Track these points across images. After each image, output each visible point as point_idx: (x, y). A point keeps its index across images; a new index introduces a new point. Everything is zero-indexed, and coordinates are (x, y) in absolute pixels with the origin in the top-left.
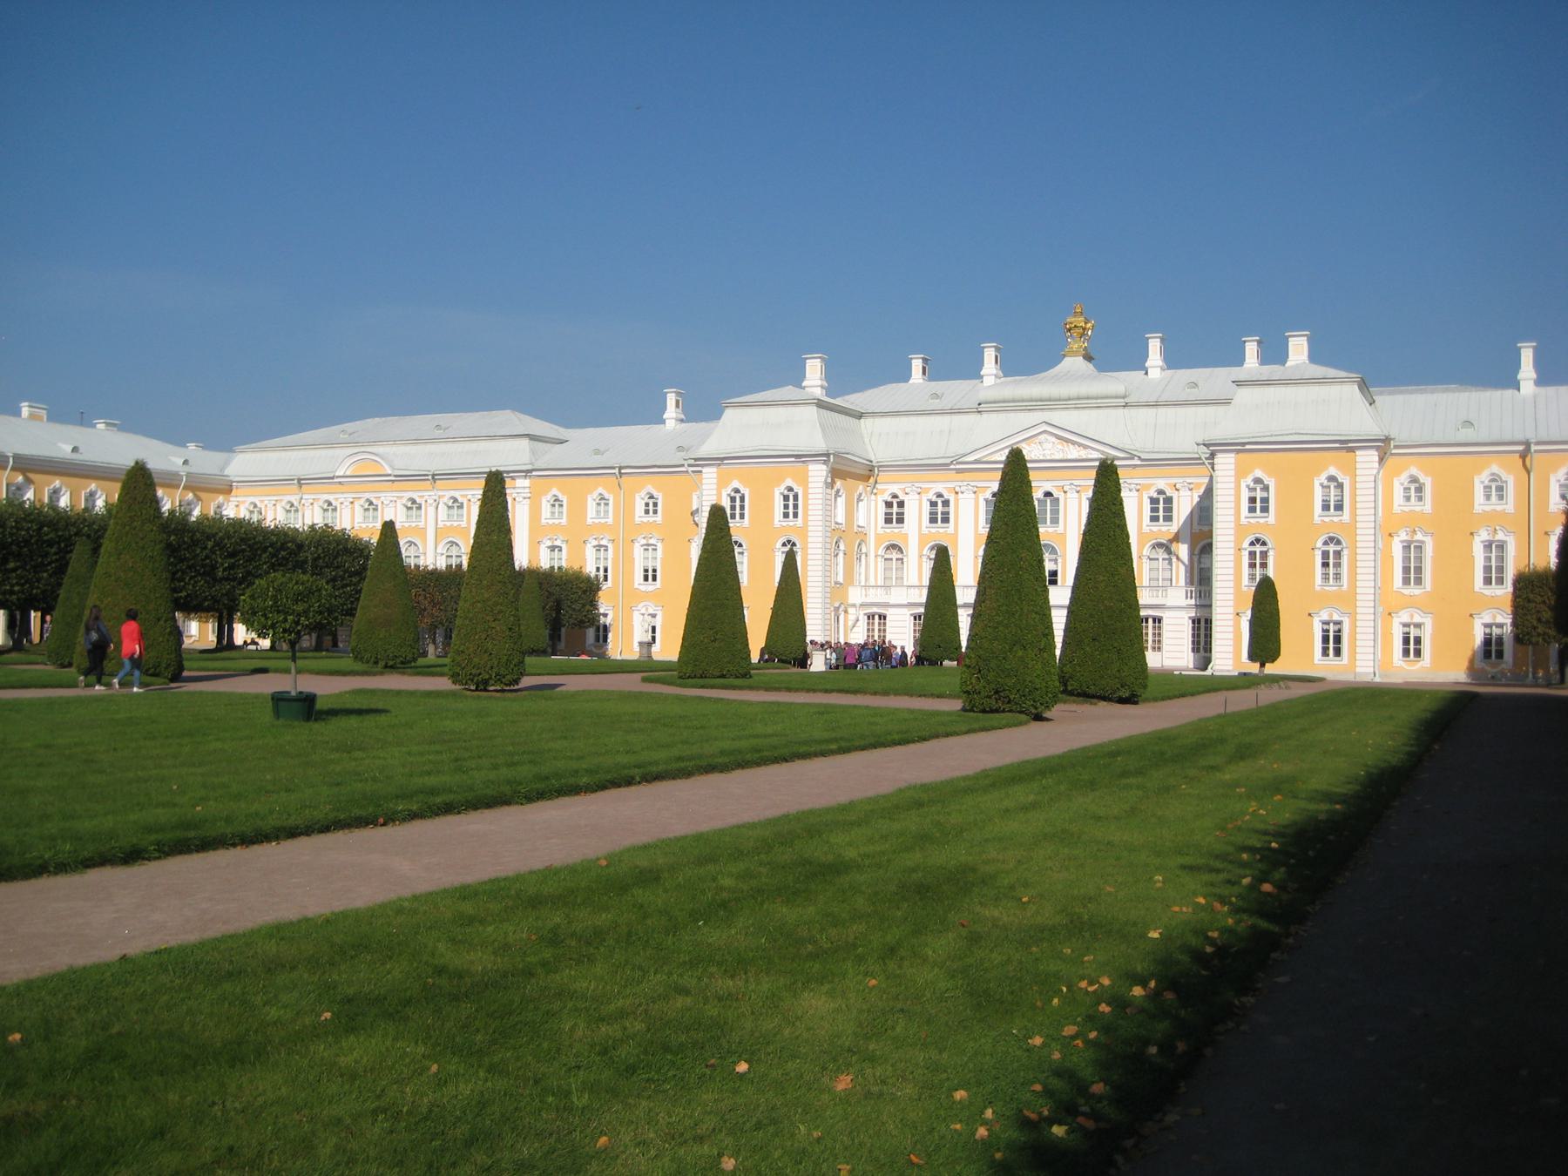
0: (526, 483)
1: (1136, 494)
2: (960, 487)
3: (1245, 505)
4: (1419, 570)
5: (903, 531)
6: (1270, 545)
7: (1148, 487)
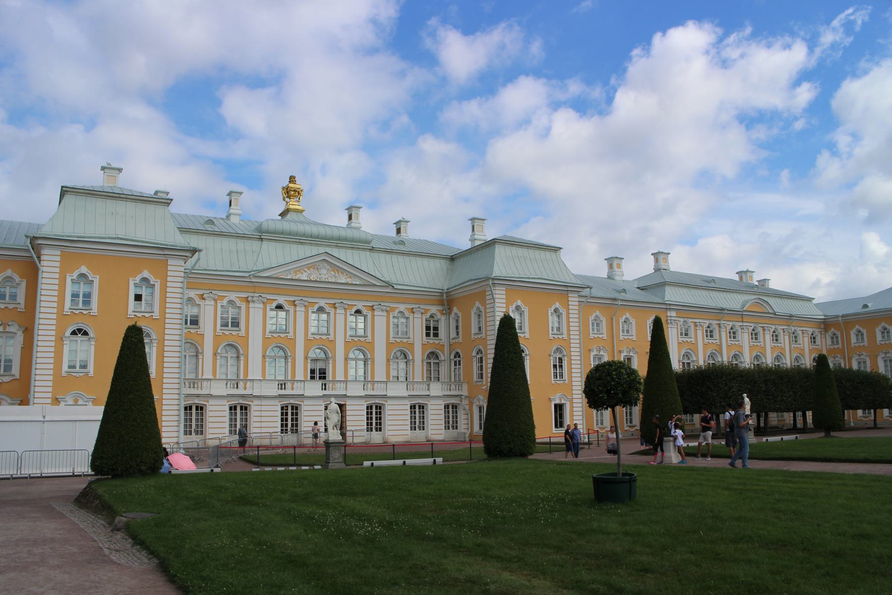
1: (385, 314)
2: (253, 297)
7: (393, 309)
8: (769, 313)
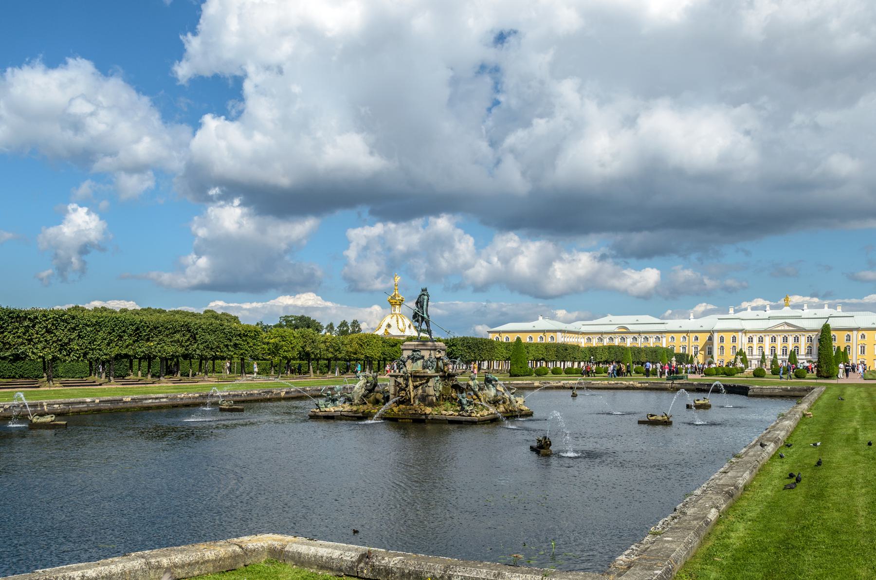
4: (864, 351)
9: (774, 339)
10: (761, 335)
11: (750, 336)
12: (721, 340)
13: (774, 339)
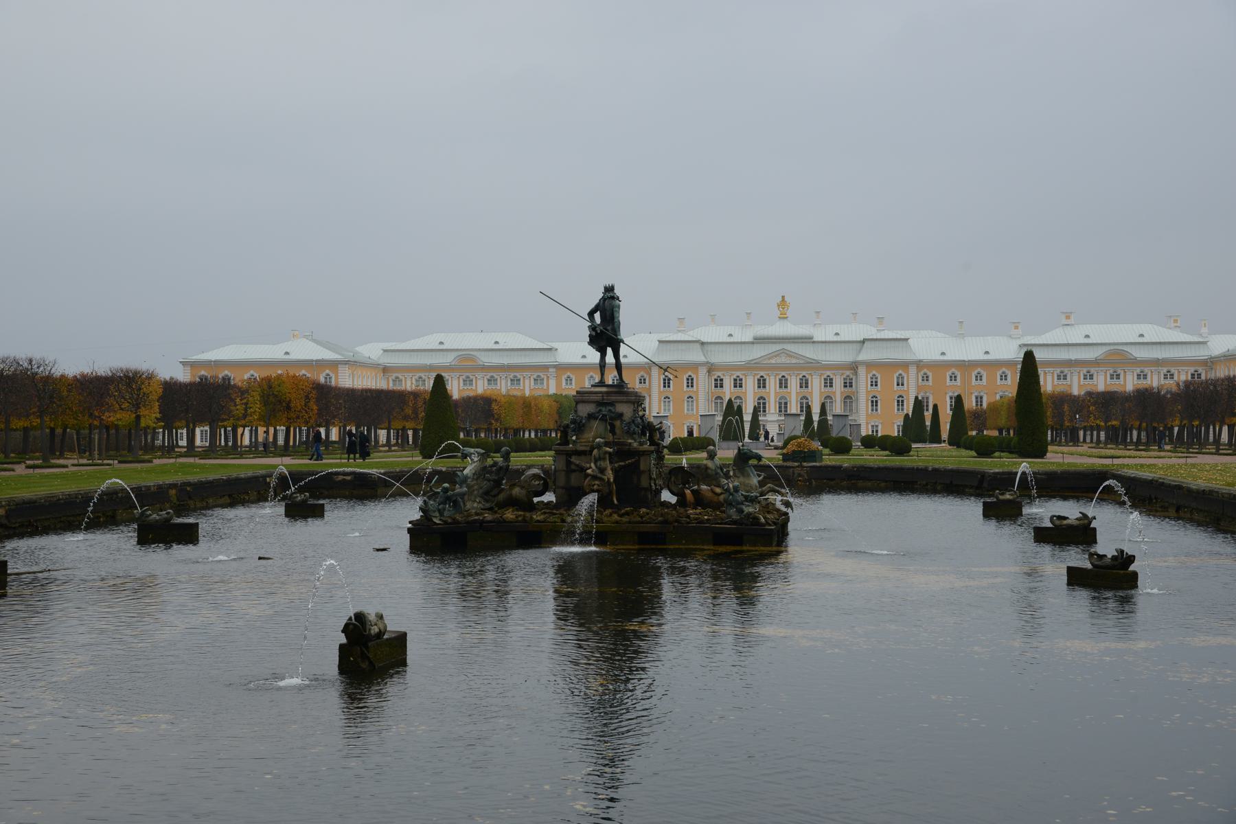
0: (554, 370)
3: (869, 383)
5: (724, 391)
6: (879, 398)
8: (1131, 359)
9: (762, 383)
10: (738, 373)
11: (719, 377)
12: (665, 383)
13: (762, 383)
